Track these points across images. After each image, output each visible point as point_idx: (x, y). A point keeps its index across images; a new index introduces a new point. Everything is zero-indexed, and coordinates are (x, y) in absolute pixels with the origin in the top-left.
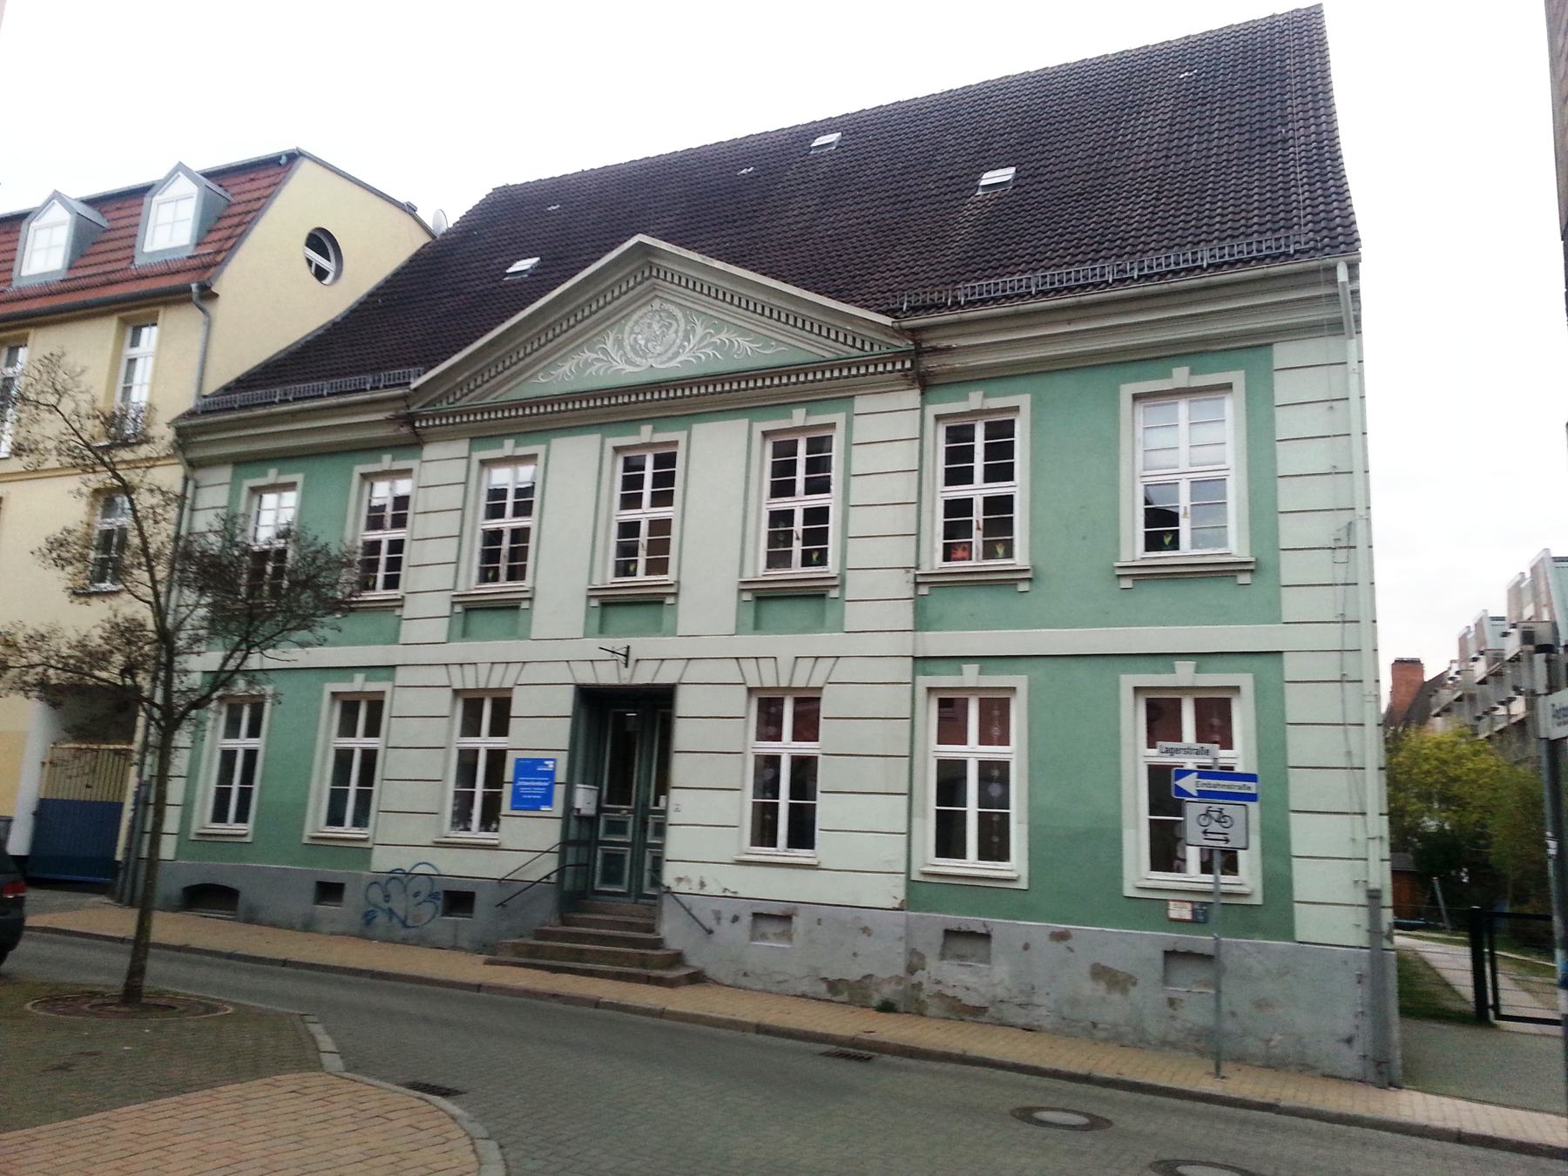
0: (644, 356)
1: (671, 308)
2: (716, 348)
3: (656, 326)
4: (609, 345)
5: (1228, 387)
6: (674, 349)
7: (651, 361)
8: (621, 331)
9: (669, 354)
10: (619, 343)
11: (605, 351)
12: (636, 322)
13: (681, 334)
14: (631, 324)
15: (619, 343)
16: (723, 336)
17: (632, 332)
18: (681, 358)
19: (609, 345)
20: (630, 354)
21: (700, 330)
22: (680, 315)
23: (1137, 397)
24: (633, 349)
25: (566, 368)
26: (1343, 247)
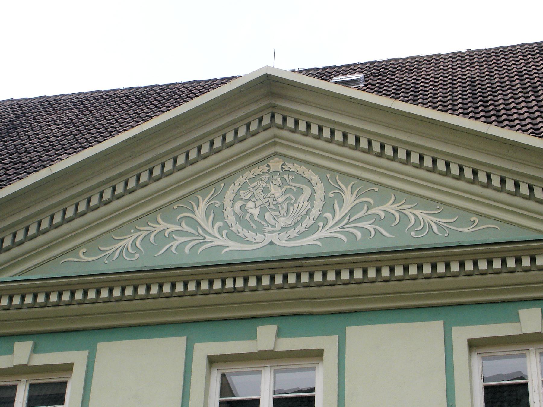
0: (259, 229)
1: (301, 169)
2: (377, 220)
3: (276, 192)
4: (200, 214)
5: (318, 354)
6: (309, 222)
7: (270, 237)
8: (221, 196)
9: (301, 228)
10: (217, 213)
11: (193, 223)
12: (244, 186)
13: (318, 204)
14: (234, 187)
15: (217, 213)
16: (389, 207)
17: (236, 198)
18: (322, 233)
19: (200, 214)
20: (236, 227)
21: (349, 200)
22: (315, 179)
23: (474, 345)
24: (240, 219)
25: (128, 242)
26: (506, 123)
